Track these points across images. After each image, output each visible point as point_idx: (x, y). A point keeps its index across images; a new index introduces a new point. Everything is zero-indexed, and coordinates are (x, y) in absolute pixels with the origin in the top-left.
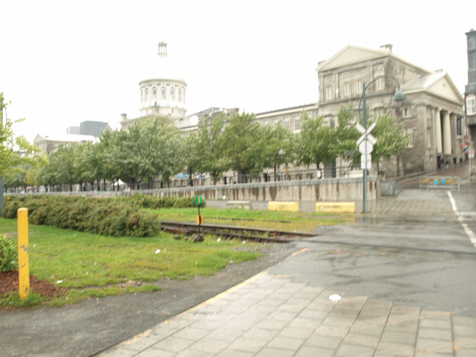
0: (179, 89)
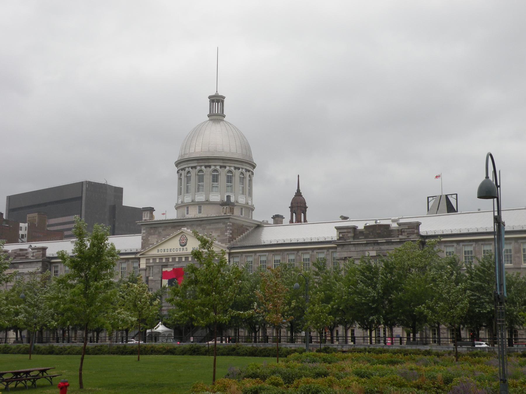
0: (242, 173)
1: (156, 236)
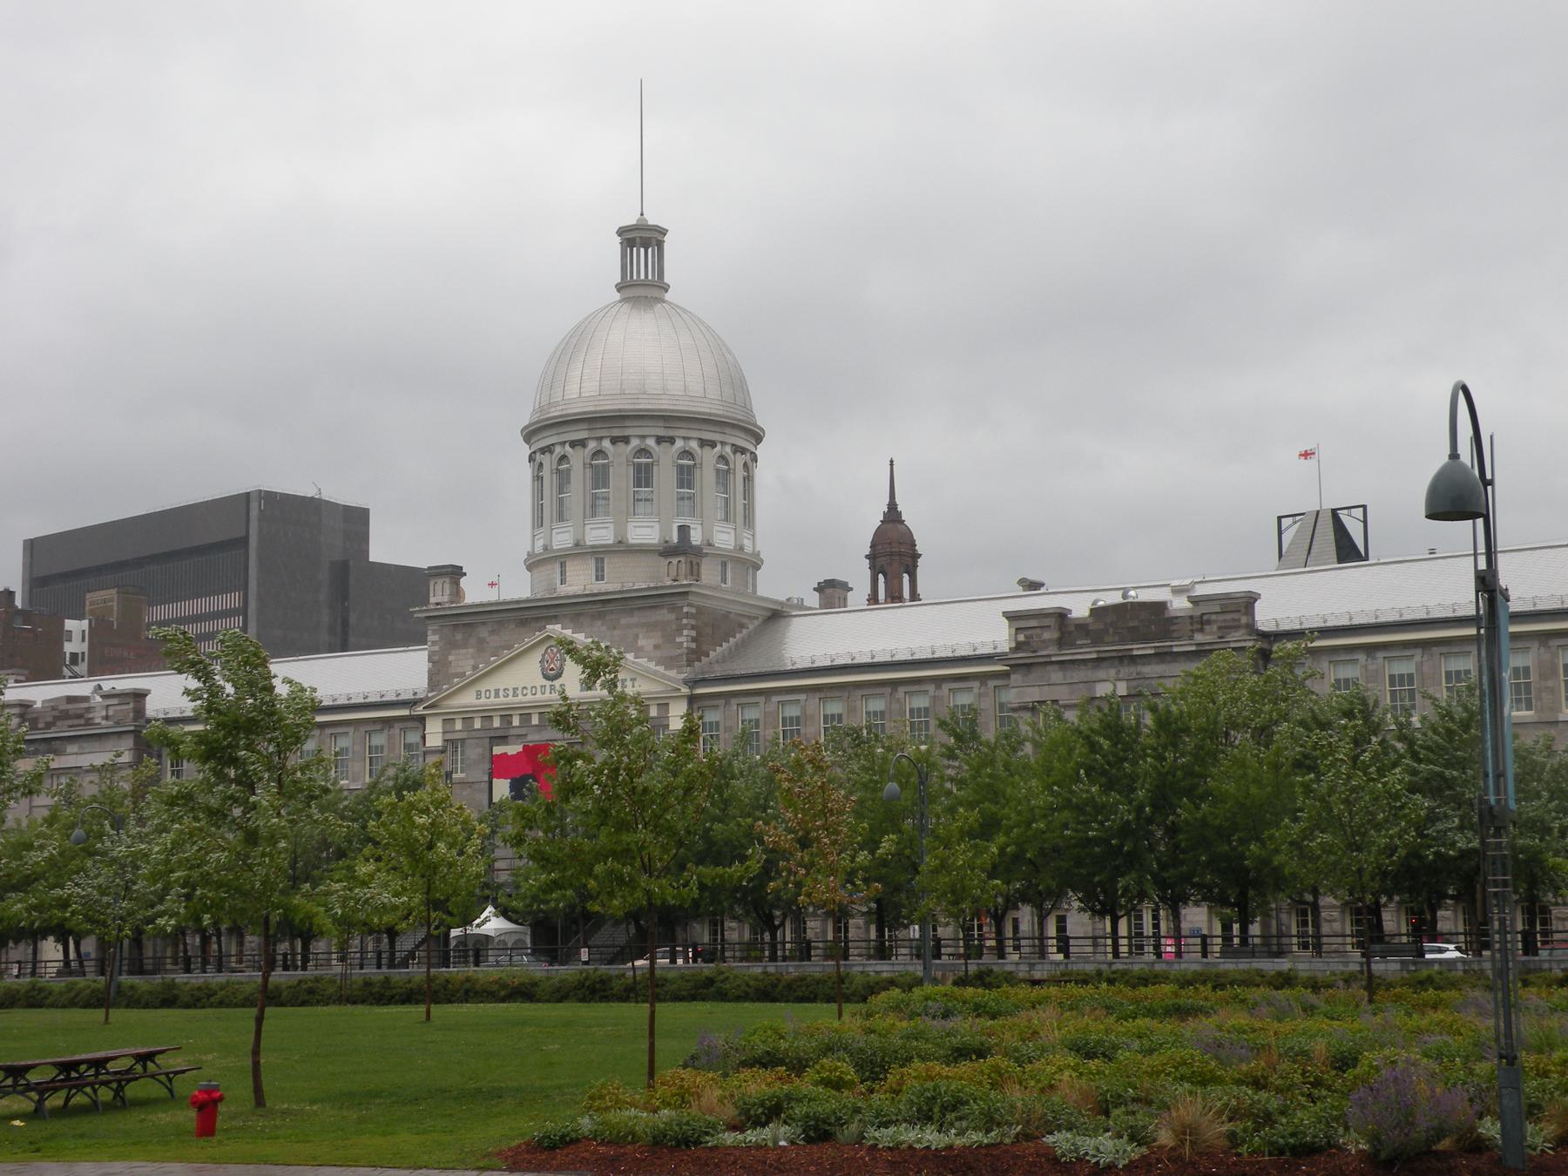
0: (722, 458)
1: (471, 650)
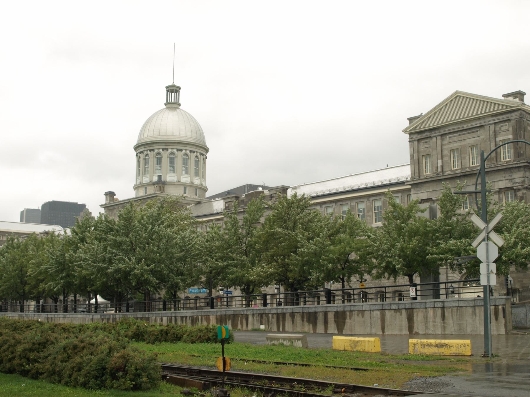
0: (197, 157)
